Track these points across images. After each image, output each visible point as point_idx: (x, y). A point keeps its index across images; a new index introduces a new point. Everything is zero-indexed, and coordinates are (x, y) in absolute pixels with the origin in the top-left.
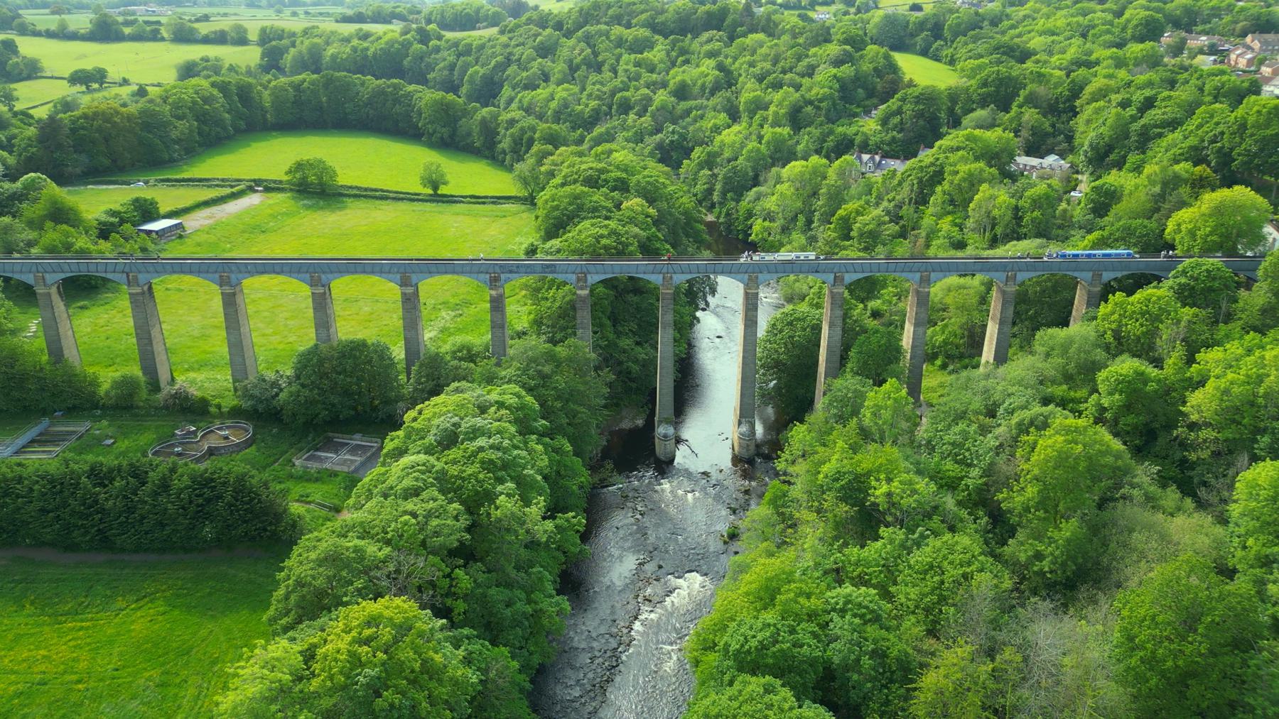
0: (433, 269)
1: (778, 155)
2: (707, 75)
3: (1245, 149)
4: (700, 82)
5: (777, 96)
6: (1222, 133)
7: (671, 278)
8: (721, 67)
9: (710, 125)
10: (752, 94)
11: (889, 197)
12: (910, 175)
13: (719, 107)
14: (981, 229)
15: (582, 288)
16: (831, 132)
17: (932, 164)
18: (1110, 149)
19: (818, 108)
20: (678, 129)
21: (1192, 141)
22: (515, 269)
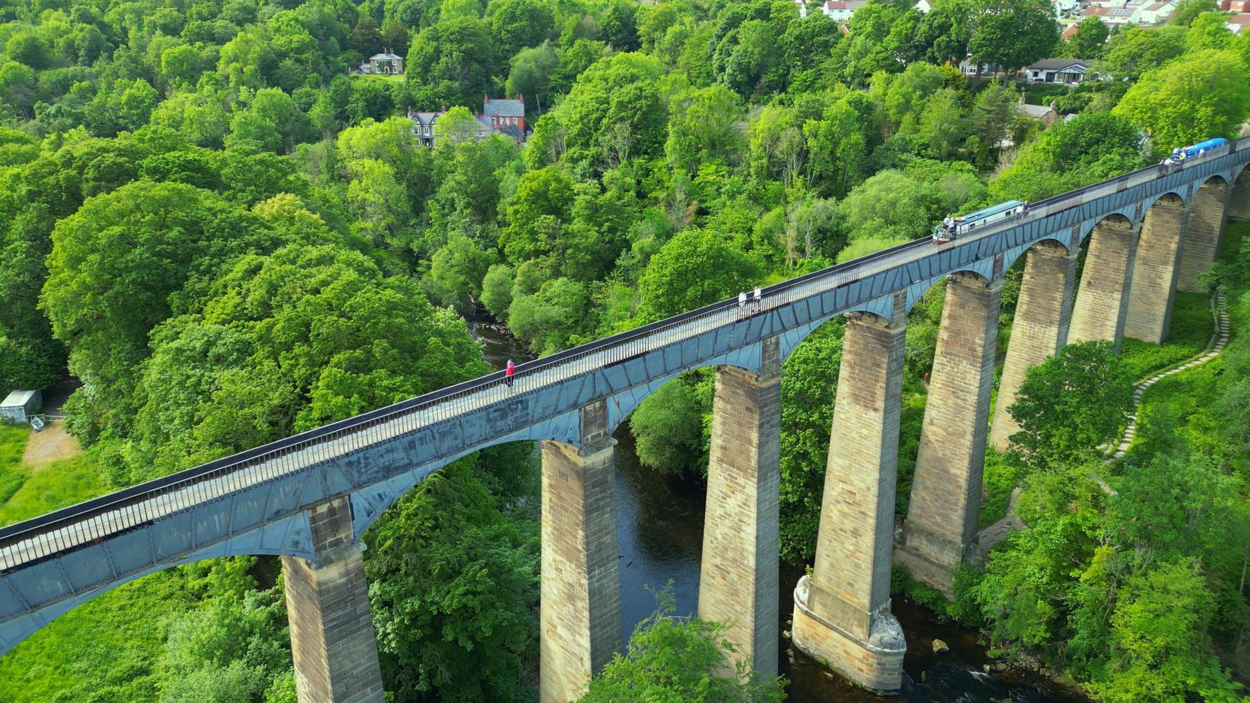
0: (48, 583)
1: (288, 127)
2: (66, 32)
3: (984, 39)
4: (61, 42)
5: (228, 48)
6: (944, 28)
7: (777, 343)
8: (86, 18)
9: (124, 98)
10: (177, 50)
11: (575, 151)
12: (599, 120)
13: (123, 71)
14: (774, 171)
15: (598, 448)
16: (350, 90)
17: (639, 98)
18: (762, 67)
19: (298, 61)
20: (65, 108)
21: (891, 41)
22: (400, 456)
